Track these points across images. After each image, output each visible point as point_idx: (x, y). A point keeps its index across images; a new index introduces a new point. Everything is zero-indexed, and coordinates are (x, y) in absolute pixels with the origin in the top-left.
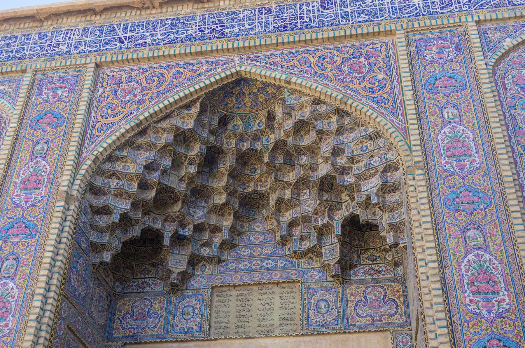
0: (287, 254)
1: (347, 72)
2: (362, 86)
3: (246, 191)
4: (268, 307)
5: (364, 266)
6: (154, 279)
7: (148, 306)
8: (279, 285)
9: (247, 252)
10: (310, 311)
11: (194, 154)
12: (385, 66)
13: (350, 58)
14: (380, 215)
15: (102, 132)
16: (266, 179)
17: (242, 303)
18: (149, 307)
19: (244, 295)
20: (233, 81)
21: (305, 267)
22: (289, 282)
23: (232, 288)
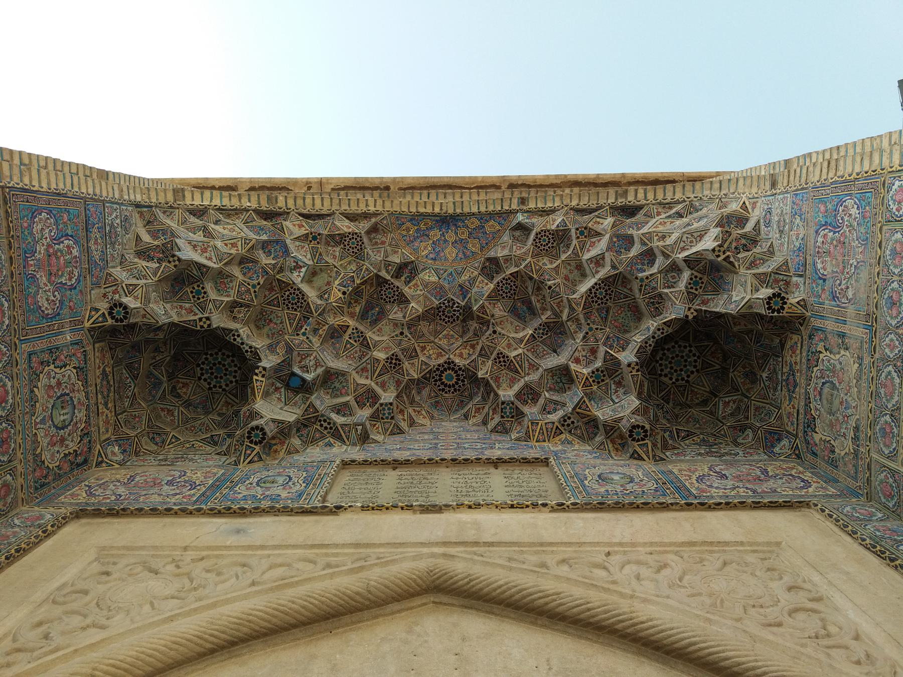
10: (586, 482)
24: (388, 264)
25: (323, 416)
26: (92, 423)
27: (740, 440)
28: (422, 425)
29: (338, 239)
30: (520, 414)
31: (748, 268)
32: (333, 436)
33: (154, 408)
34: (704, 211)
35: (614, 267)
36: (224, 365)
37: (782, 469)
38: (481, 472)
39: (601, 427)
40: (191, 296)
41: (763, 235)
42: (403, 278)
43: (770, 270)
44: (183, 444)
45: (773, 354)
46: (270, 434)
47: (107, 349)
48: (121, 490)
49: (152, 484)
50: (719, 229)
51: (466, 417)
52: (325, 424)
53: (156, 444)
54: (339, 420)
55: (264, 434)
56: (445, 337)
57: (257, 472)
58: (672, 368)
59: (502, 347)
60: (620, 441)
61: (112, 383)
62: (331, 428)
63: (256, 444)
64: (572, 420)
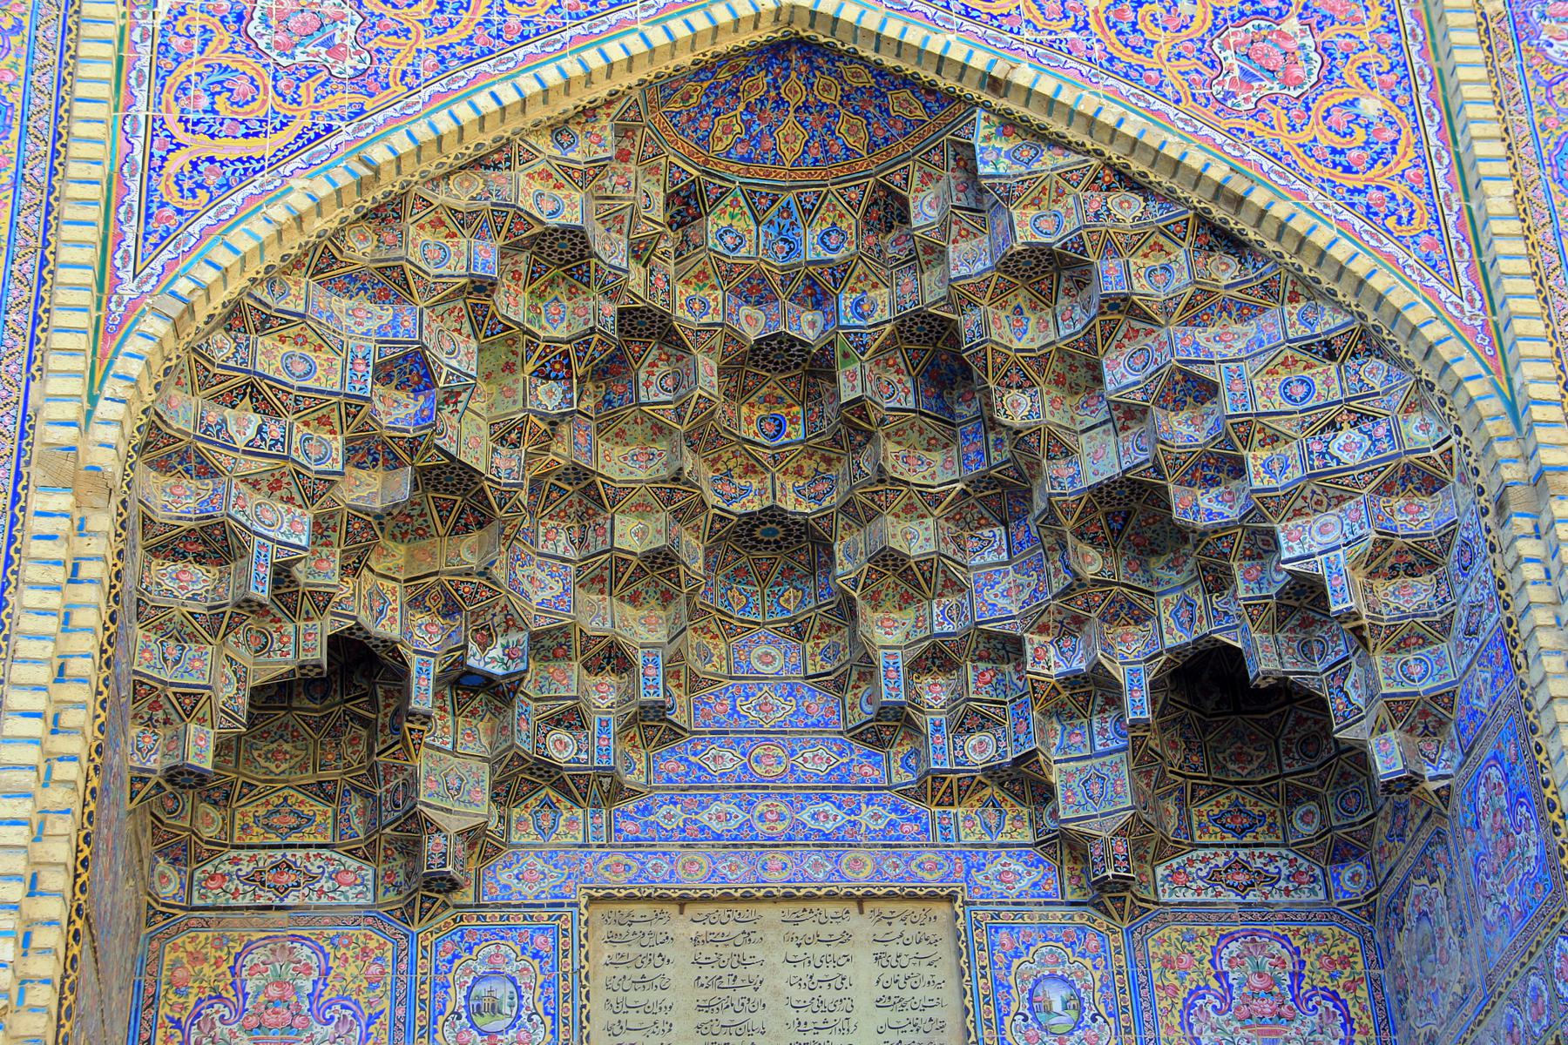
0: (895, 780)
1: (1237, 72)
2: (1304, 137)
3: (735, 508)
4: (829, 995)
5: (1209, 852)
6: (326, 853)
7: (308, 968)
8: (868, 907)
9: (728, 760)
10: (1007, 1020)
11: (565, 335)
12: (1386, 67)
13: (1242, 14)
14: (1332, 659)
15: (203, 195)
16: (823, 467)
17: (717, 972)
18: (315, 975)
19: (726, 940)
20: (754, 45)
21: (972, 839)
22: (912, 897)
23: (673, 909)
32: (554, 786)
56: (765, 400)
63: (439, 892)
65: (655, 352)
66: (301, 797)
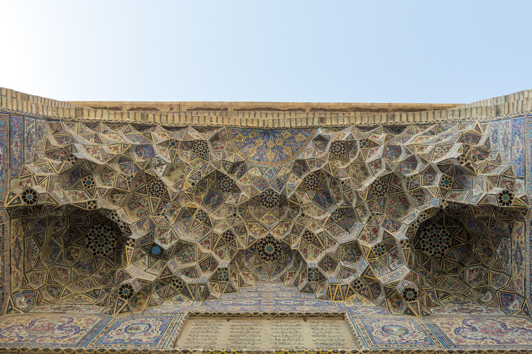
10: (373, 333)
24: (225, 163)
25: (175, 277)
26: (6, 279)
27: (483, 300)
28: (249, 285)
29: (190, 145)
30: (321, 279)
31: (483, 172)
32: (183, 293)
33: (53, 268)
34: (449, 130)
35: (388, 169)
36: (105, 237)
37: (517, 323)
38: (294, 324)
39: (382, 289)
40: (83, 185)
41: (492, 149)
42: (236, 174)
43: (499, 174)
44: (73, 296)
45: (504, 236)
46: (136, 291)
47: (20, 223)
48: (24, 333)
49: (47, 328)
50: (461, 143)
51: (282, 279)
52: (177, 284)
53: (53, 296)
54: (188, 280)
55: (132, 291)
57: (125, 320)
58: (431, 244)
59: (308, 226)
60: (396, 300)
61: (22, 249)
62: (181, 287)
63: (125, 298)
64: (361, 283)
65: (231, 196)
66: (86, 297)
